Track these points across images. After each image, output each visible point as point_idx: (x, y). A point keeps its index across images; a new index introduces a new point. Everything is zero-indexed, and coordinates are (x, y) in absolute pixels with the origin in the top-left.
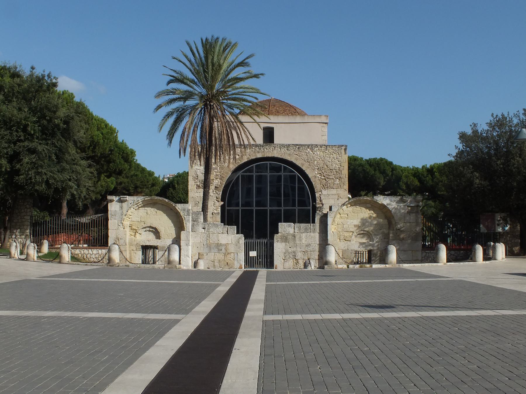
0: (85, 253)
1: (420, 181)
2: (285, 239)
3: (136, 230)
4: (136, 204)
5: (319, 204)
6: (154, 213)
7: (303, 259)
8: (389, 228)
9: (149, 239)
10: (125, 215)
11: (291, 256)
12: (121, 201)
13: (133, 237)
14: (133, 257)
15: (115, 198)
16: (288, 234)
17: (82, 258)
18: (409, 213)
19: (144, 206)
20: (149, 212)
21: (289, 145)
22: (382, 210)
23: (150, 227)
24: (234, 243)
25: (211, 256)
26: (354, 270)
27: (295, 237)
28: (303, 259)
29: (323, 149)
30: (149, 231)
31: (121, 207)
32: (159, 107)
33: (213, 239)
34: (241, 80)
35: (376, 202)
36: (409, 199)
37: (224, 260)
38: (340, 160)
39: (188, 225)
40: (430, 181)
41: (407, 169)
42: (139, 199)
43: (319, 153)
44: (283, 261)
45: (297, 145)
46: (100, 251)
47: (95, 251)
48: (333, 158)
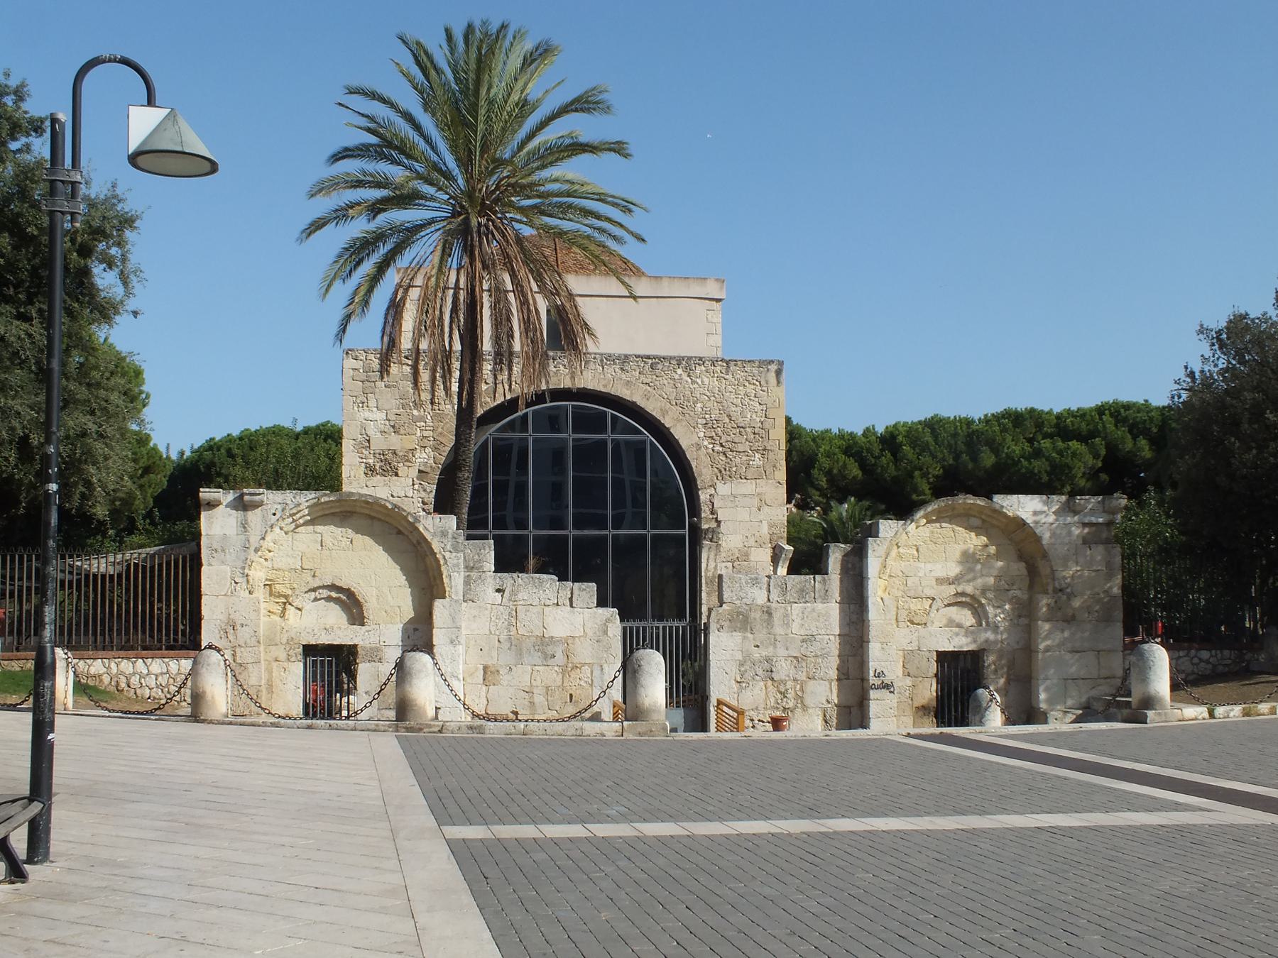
0: (122, 673)
1: (863, 467)
2: (741, 621)
3: (286, 597)
4: (291, 515)
5: (708, 520)
6: (346, 542)
7: (795, 680)
8: (1031, 587)
9: (329, 626)
10: (256, 550)
11: (760, 672)
12: (242, 505)
13: (278, 619)
14: (276, 682)
15: (227, 497)
16: (751, 607)
17: (112, 689)
18: (1086, 541)
19: (311, 522)
20: (328, 540)
21: (626, 357)
22: (1016, 537)
23: (333, 587)
24: (590, 633)
25: (523, 675)
26: (1228, 727)
27: (769, 614)
28: (795, 680)
29: (718, 369)
30: (329, 599)
31: (244, 526)
32: (318, 225)
33: (529, 623)
34: (585, 151)
35: (999, 513)
36: (1091, 502)
37: (563, 687)
38: (764, 400)
39: (454, 579)
40: (892, 469)
41: (824, 436)
42: (306, 498)
43: (707, 381)
44: (735, 686)
45: (648, 357)
46: (173, 665)
47: (156, 666)
48: (746, 394)
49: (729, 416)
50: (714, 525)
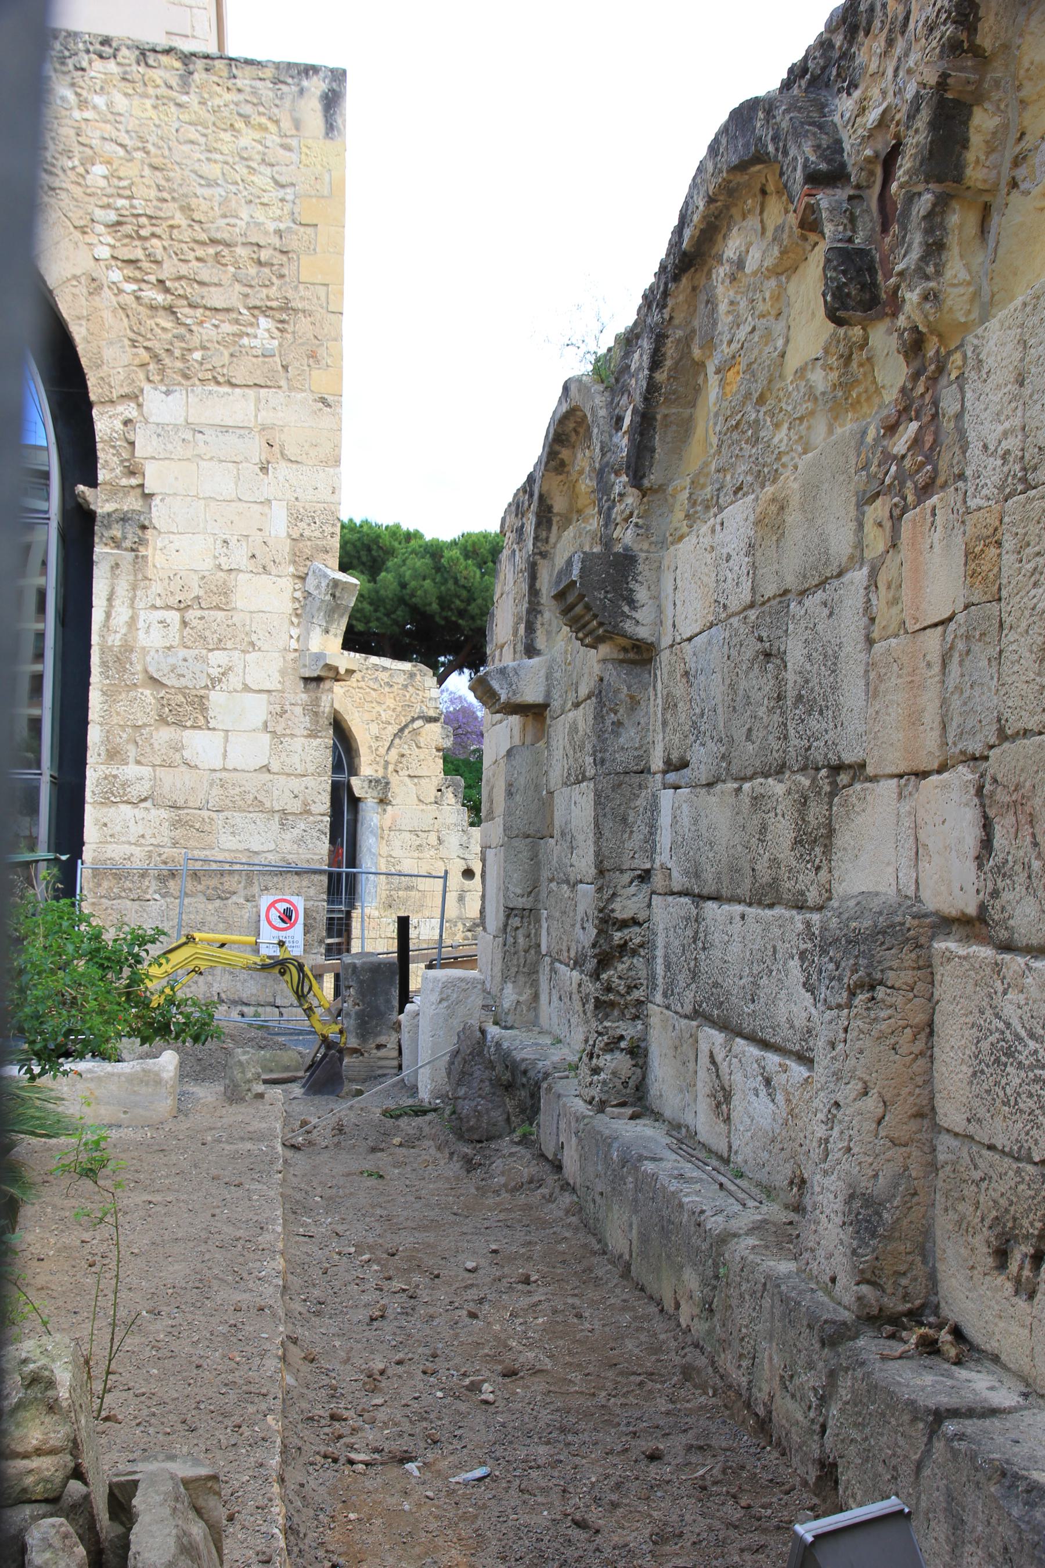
5: (116, 490)
29: (157, 75)
49: (187, 209)
50: (132, 503)
